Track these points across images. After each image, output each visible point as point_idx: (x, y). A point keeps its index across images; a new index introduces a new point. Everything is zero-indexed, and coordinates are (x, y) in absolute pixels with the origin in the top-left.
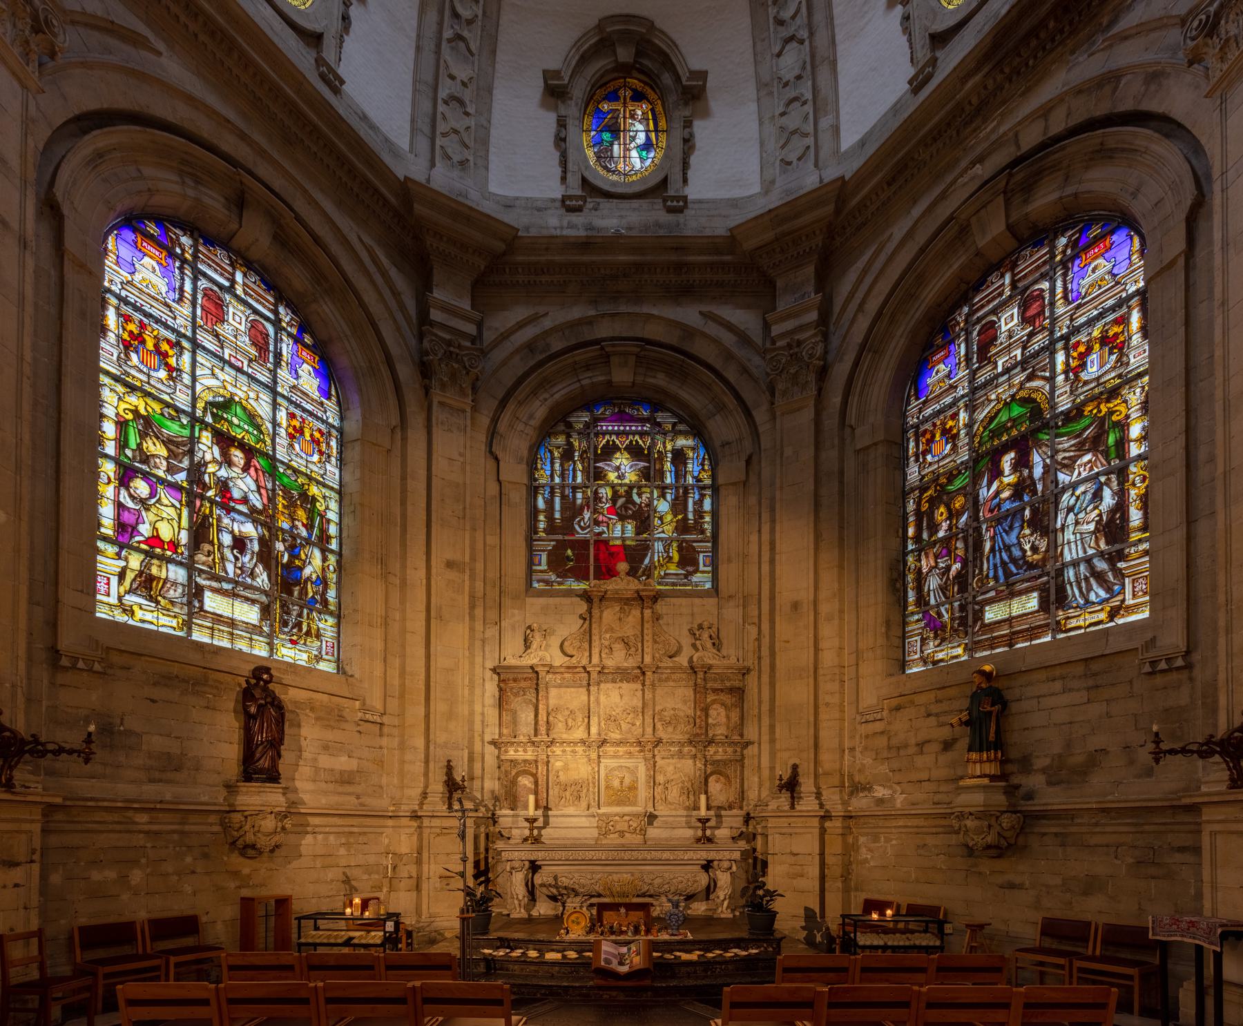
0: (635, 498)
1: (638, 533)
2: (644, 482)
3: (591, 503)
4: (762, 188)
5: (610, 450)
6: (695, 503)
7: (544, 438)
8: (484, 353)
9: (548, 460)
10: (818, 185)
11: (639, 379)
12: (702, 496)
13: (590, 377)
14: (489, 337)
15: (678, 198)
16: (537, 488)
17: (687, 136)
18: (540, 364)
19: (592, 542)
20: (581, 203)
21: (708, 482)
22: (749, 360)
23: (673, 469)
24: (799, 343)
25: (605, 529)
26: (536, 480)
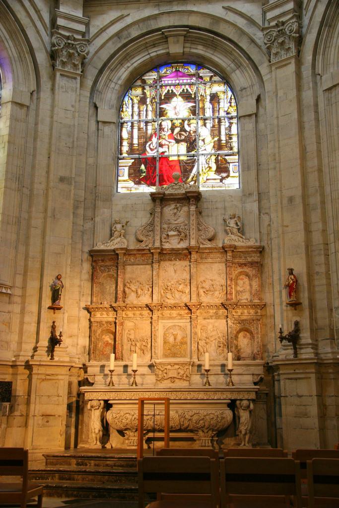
0: (187, 128)
1: (188, 152)
2: (192, 117)
3: (158, 132)
5: (169, 97)
6: (226, 129)
7: (127, 91)
8: (89, 42)
9: (130, 105)
11: (187, 50)
12: (231, 124)
13: (156, 51)
14: (93, 31)
16: (122, 124)
18: (125, 45)
19: (158, 159)
21: (234, 114)
22: (255, 35)
23: (211, 106)
24: (283, 23)
25: (167, 150)
26: (122, 119)
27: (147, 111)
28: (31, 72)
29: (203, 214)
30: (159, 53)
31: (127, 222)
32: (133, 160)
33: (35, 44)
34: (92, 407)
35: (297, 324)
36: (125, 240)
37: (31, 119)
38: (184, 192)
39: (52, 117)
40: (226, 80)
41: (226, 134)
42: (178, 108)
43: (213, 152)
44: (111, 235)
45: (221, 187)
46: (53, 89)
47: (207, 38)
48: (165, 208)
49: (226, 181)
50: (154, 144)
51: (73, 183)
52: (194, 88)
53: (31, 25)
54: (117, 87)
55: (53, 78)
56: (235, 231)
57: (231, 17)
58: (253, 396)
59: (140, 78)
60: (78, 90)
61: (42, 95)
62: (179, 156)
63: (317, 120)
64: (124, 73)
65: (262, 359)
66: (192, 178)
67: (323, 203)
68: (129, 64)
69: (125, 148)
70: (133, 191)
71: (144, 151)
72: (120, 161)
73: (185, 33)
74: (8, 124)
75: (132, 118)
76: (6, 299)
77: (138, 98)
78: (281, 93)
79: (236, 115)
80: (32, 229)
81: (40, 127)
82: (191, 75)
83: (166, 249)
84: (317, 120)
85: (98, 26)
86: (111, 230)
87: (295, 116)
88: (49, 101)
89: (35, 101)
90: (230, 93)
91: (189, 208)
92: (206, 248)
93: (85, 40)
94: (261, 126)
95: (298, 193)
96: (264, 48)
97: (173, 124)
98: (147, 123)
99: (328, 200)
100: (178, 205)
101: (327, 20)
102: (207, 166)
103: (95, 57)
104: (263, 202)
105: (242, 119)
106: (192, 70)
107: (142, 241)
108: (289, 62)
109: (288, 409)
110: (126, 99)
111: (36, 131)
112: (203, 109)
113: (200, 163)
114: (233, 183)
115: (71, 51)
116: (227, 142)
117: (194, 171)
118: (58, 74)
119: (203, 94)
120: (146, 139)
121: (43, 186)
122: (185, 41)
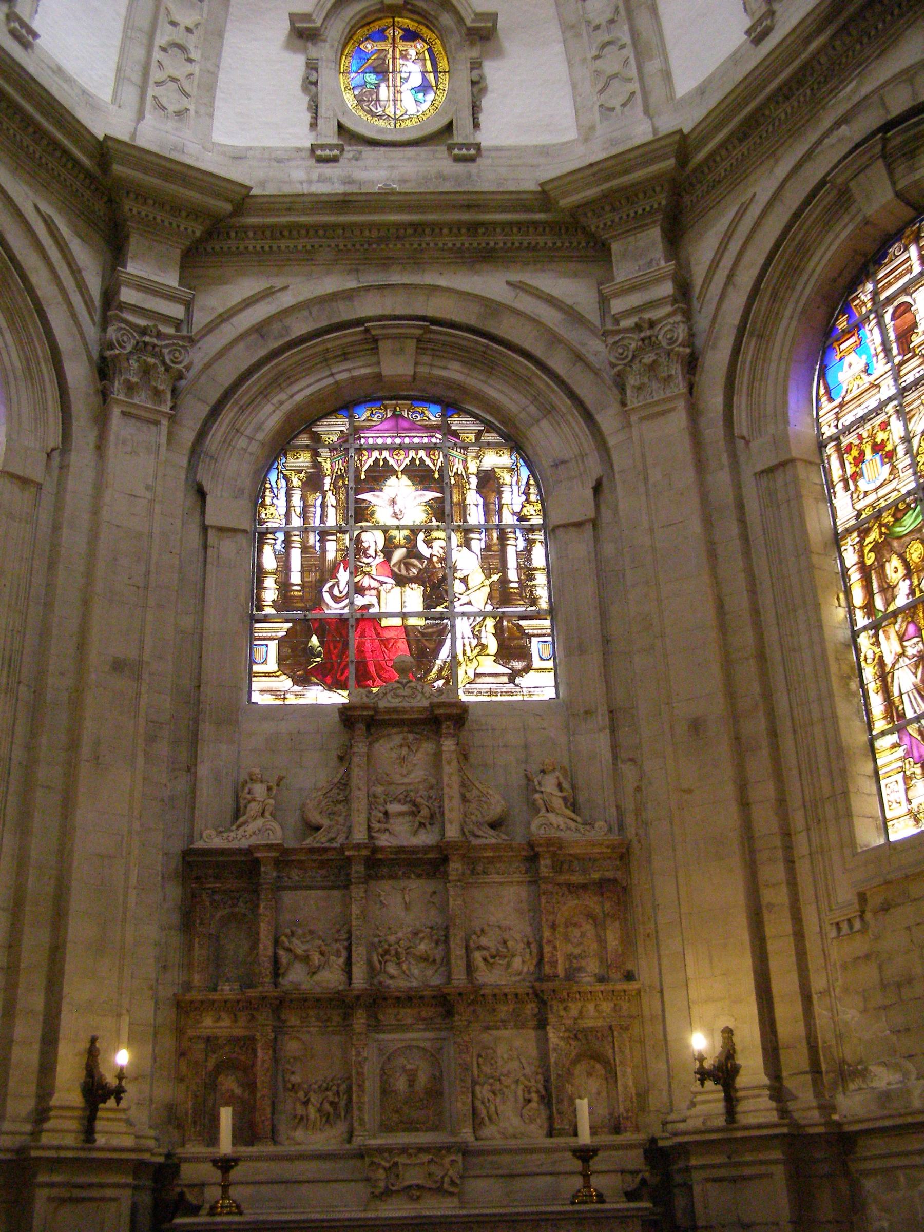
2: (435, 523)
3: (351, 558)
4: (579, 134)
6: (518, 555)
7: (276, 459)
8: (192, 341)
9: (282, 493)
10: (650, 137)
11: (423, 370)
12: (530, 543)
13: (348, 370)
14: (200, 319)
15: (468, 146)
16: (262, 535)
17: (475, 78)
18: (276, 353)
19: (352, 622)
20: (336, 152)
21: (537, 520)
22: (584, 345)
23: (481, 501)
24: (652, 324)
25: (374, 601)
27: (323, 506)
28: (50, 403)
29: (472, 759)
30: (356, 373)
31: (281, 779)
32: (290, 625)
33: (66, 341)
35: (728, 1033)
36: (275, 826)
37: (45, 517)
38: (426, 703)
39: (95, 512)
41: (519, 567)
43: (489, 608)
44: (237, 813)
45: (511, 694)
46: (100, 447)
47: (472, 345)
48: (376, 745)
49: (525, 681)
50: (342, 585)
51: (145, 676)
53: (60, 298)
54: (254, 447)
55: (101, 420)
56: (558, 803)
57: (526, 304)
59: (308, 429)
60: (163, 449)
61: (74, 458)
62: (404, 616)
63: (745, 538)
65: (637, 1129)
66: (441, 670)
67: (773, 733)
68: (282, 396)
69: (270, 594)
70: (291, 700)
71: (318, 602)
72: (257, 625)
73: (420, 332)
75: (288, 521)
77: (303, 474)
78: (655, 475)
79: (541, 522)
80: (39, 793)
82: (432, 426)
83: (383, 849)
84: (745, 538)
85: (213, 309)
86: (237, 798)
87: (696, 526)
88: (89, 474)
89: (55, 474)
90: (524, 473)
91: (439, 745)
92: (485, 847)
93: (183, 338)
94: (609, 549)
96: (609, 375)
99: (785, 726)
100: (411, 737)
101: (754, 322)
102: (474, 642)
103: (204, 377)
105: (560, 532)
106: (433, 415)
107: (317, 828)
108: (668, 406)
110: (273, 476)
111: (55, 547)
112: (463, 506)
113: (459, 635)
115: (151, 361)
118: (116, 411)
119: (461, 470)
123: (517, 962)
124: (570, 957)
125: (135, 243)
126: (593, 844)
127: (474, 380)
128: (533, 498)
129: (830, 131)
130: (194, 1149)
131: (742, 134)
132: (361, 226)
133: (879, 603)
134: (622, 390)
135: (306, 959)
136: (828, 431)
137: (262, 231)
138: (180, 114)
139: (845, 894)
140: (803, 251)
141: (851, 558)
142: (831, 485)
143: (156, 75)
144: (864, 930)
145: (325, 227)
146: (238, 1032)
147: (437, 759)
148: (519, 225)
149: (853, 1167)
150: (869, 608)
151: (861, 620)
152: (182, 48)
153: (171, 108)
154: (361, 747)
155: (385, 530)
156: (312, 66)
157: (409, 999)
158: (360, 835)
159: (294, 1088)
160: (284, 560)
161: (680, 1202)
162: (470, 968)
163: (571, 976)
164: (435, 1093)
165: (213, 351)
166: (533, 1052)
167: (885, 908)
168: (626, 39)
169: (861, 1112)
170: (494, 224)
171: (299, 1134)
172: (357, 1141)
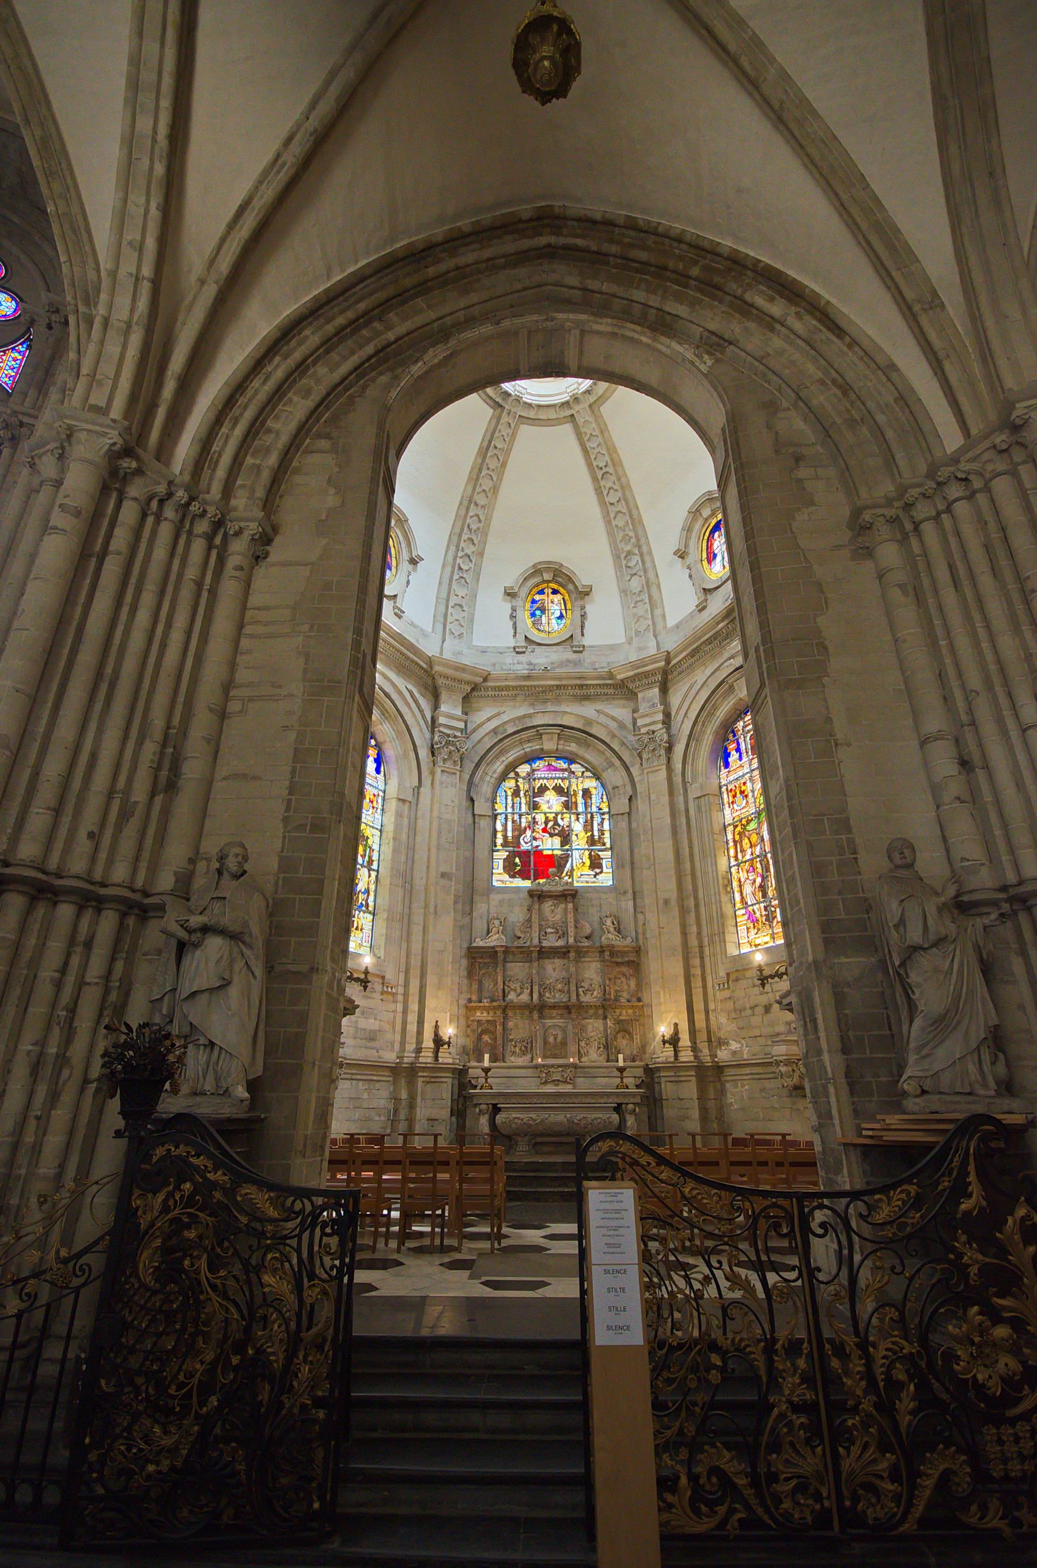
0: (560, 821)
1: (562, 846)
5: (543, 790)
11: (560, 747)
12: (603, 819)
14: (470, 727)
21: (606, 810)
24: (654, 732)
34: (480, 1111)
35: (676, 1025)
40: (597, 777)
42: (551, 802)
44: (488, 932)
52: (567, 782)
54: (493, 780)
55: (432, 773)
56: (612, 929)
57: (602, 719)
58: (638, 1100)
59: (514, 770)
61: (422, 789)
64: (499, 767)
67: (697, 906)
68: (504, 758)
69: (500, 840)
70: (508, 885)
71: (518, 845)
74: (393, 819)
76: (391, 998)
78: (653, 797)
81: (420, 822)
87: (668, 820)
90: (601, 789)
95: (673, 895)
97: (547, 818)
98: (520, 816)
104: (638, 901)
106: (562, 764)
109: (670, 1112)
112: (576, 803)
114: (606, 879)
116: (600, 838)
117: (568, 865)
118: (438, 771)
120: (519, 831)
121: (424, 882)
122: (559, 739)
123: (595, 993)
124: (616, 991)
125: (444, 696)
126: (626, 947)
127: (581, 751)
128: (605, 800)
129: (726, 661)
130: (474, 1064)
131: (692, 654)
132: (535, 687)
133: (740, 856)
134: (641, 758)
135: (515, 990)
136: (723, 782)
137: (494, 688)
138: (461, 635)
139: (722, 973)
140: (715, 708)
141: (730, 836)
142: (723, 804)
143: (450, 619)
144: (728, 988)
145: (520, 686)
146: (490, 1018)
147: (566, 909)
148: (600, 685)
149: (723, 1079)
150: (736, 857)
151: (733, 862)
152: (461, 606)
153: (456, 634)
154: (536, 906)
155: (545, 814)
156: (514, 609)
157: (554, 1007)
158: (536, 941)
159: (511, 1040)
160: (505, 826)
161: (657, 1089)
162: (578, 995)
163: (616, 999)
164: (564, 1043)
165: (476, 740)
166: (602, 1029)
167: (737, 980)
168: (647, 601)
169: (726, 1058)
170: (590, 685)
171: (512, 1059)
172: (535, 1062)
